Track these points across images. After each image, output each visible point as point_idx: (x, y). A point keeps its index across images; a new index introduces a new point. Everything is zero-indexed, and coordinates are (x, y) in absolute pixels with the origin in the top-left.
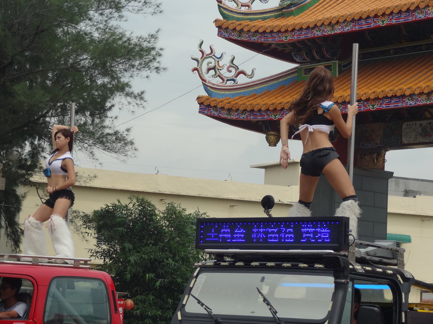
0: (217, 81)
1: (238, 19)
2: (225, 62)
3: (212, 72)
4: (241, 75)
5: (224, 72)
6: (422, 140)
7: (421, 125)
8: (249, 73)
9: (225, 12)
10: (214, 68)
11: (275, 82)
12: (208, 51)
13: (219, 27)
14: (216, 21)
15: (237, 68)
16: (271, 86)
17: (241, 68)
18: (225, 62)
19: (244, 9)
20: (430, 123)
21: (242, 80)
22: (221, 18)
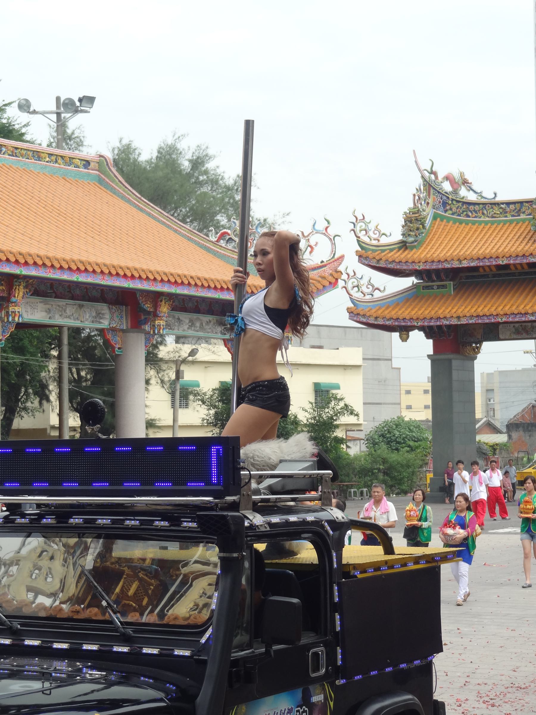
0: (359, 295)
1: (373, 250)
2: (364, 281)
3: (356, 289)
4: (377, 291)
5: (364, 289)
6: (515, 337)
7: (514, 326)
8: (382, 289)
9: (364, 245)
10: (357, 286)
11: (401, 296)
12: (352, 274)
13: (360, 256)
14: (357, 252)
15: (373, 286)
16: (399, 298)
17: (376, 286)
18: (364, 281)
19: (375, 242)
20: (521, 326)
21: (377, 295)
22: (360, 249)
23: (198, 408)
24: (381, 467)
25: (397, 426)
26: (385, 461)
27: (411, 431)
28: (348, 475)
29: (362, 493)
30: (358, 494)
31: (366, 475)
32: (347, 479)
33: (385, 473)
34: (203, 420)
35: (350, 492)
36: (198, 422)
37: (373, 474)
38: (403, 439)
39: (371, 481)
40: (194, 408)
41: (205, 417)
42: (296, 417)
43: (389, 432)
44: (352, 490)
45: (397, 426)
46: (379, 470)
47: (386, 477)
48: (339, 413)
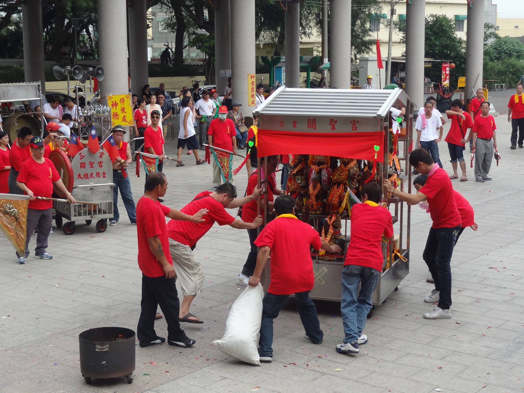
23: (398, 32)
24: (512, 70)
25: (505, 43)
26: (514, 66)
27: (515, 46)
28: (491, 75)
29: (502, 86)
30: (499, 87)
31: (502, 75)
32: (490, 77)
33: (513, 74)
34: (401, 40)
35: (494, 86)
36: (399, 41)
37: (506, 74)
38: (509, 51)
39: (505, 78)
40: (396, 33)
41: (402, 38)
42: (461, 39)
43: (500, 47)
44: (496, 85)
45: (505, 43)
46: (510, 72)
47: (514, 76)
48: (489, 36)
